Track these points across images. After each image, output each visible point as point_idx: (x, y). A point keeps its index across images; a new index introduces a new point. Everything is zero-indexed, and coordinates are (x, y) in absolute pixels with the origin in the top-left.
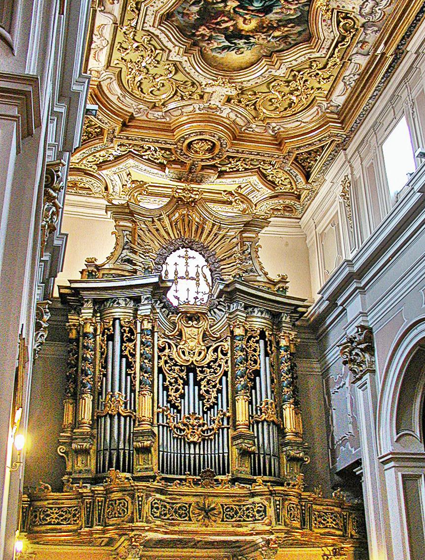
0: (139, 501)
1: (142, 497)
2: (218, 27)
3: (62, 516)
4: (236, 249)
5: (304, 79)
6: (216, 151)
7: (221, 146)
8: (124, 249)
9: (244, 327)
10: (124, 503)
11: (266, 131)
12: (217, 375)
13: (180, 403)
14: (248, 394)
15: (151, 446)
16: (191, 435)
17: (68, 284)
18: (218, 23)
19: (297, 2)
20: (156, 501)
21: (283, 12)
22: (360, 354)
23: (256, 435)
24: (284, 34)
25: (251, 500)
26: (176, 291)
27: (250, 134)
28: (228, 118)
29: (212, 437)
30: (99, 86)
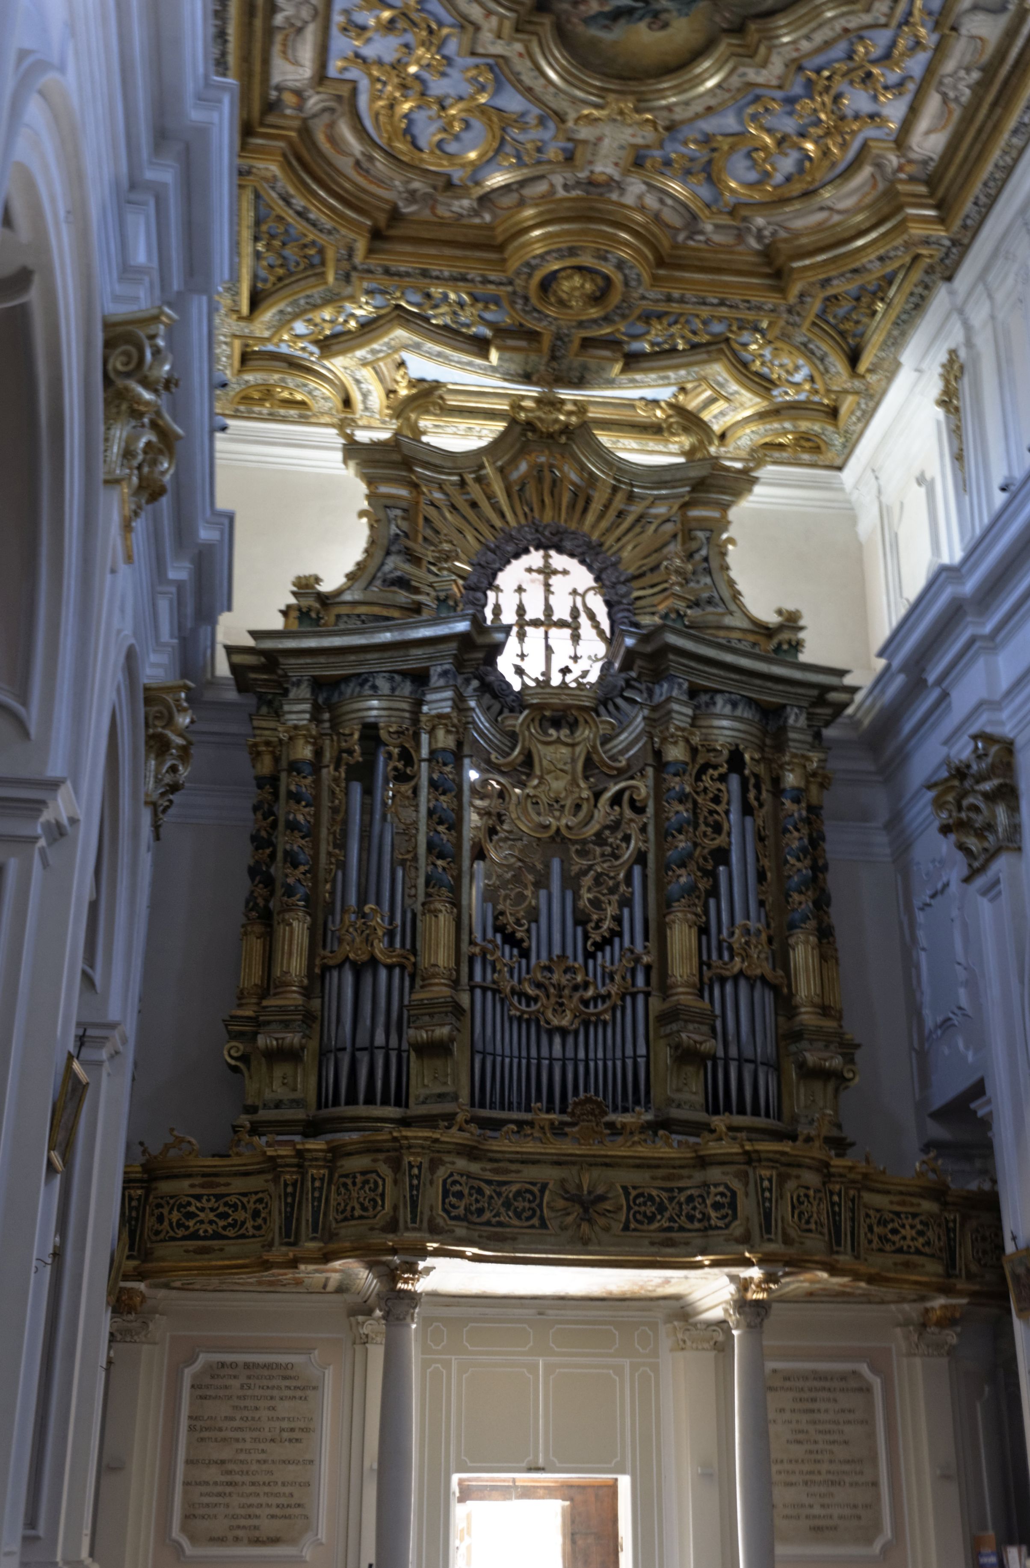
0: (411, 1177)
1: (420, 1167)
3: (224, 1216)
4: (671, 548)
5: (833, 92)
6: (615, 298)
7: (626, 284)
8: (388, 553)
9: (687, 741)
10: (376, 1183)
11: (740, 237)
12: (621, 861)
13: (528, 931)
14: (699, 910)
15: (452, 1040)
16: (554, 1010)
17: (250, 642)
20: (456, 1177)
22: (982, 806)
23: (718, 1011)
25: (699, 1176)
26: (522, 656)
27: (699, 250)
28: (642, 208)
29: (607, 1017)
30: (305, 131)
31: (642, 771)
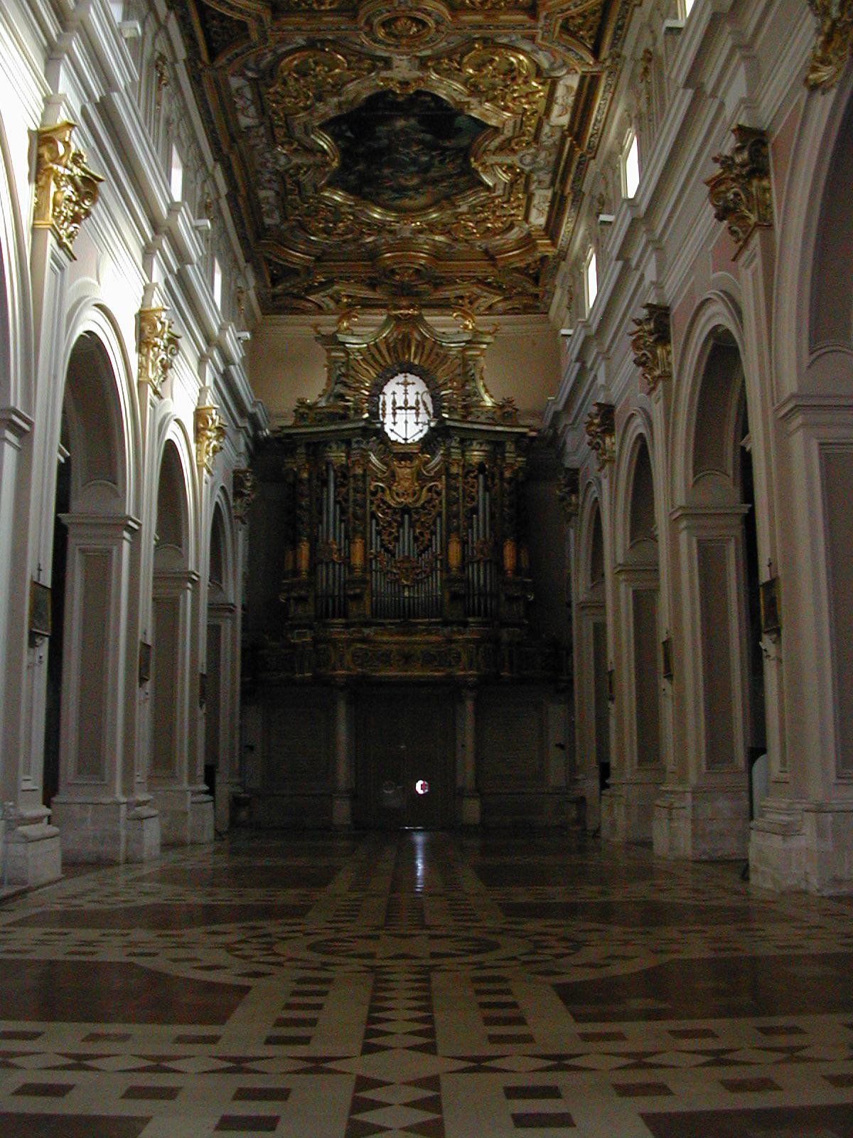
13: (395, 547)
26: (395, 423)
31: (440, 477)
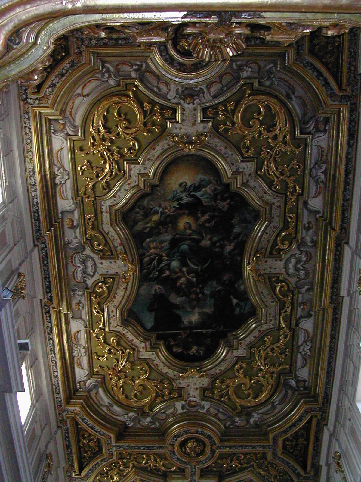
2: (212, 214)
11: (116, 67)
18: (212, 218)
19: (152, 257)
21: (160, 243)
24: (149, 218)
